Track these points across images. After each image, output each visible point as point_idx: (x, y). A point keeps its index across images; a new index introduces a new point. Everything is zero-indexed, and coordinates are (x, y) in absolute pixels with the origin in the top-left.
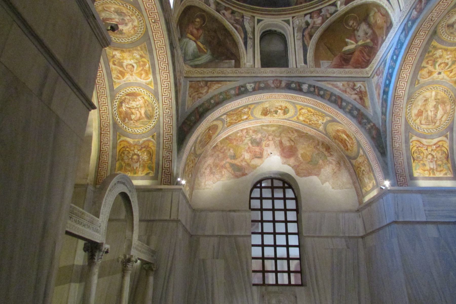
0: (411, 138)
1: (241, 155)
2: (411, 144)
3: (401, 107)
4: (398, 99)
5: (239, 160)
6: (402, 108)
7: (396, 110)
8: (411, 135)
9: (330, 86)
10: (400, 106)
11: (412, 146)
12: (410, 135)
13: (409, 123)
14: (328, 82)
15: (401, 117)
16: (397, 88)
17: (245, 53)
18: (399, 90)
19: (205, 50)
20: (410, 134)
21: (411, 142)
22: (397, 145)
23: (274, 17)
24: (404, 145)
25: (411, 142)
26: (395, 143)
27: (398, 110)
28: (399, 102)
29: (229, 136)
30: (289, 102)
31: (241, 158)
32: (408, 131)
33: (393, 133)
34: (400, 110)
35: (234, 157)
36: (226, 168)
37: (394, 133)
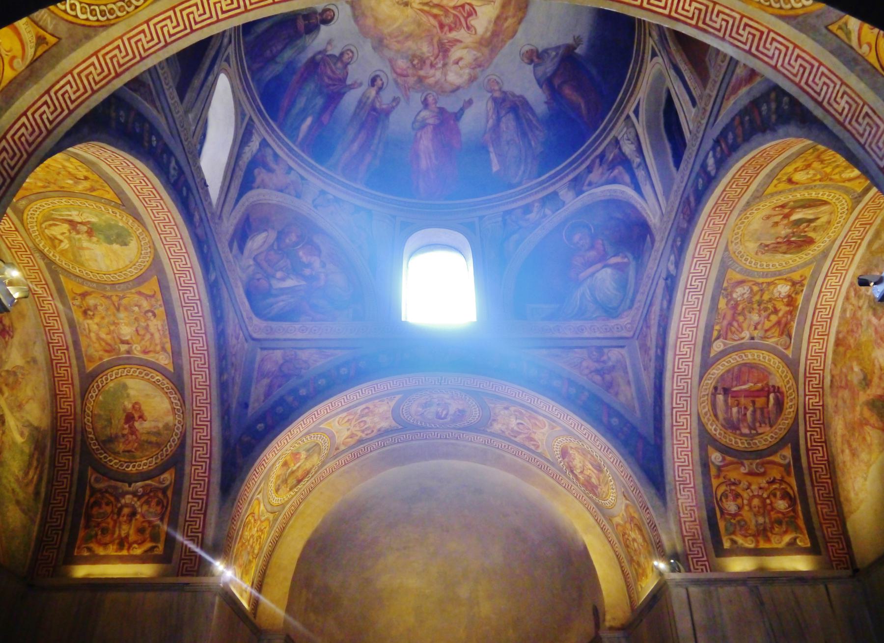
0: (848, 34)
1: (874, 365)
2: (865, 49)
3: (738, 17)
4: (711, 19)
5: (876, 380)
6: (743, 16)
7: (744, 39)
8: (840, 28)
9: (732, 101)
10: (734, 19)
11: (873, 53)
12: (839, 33)
13: (801, 12)
14: (726, 97)
15: (770, 31)
16: (673, 14)
17: (644, 205)
18: (680, 10)
19: (626, 260)
20: (834, 28)
21: (860, 45)
22: (843, 103)
23: (643, 70)
24: (853, 80)
25: (860, 45)
26: (835, 106)
27: (745, 34)
28: (719, 20)
29: (838, 332)
30: (748, 204)
31: (876, 371)
32: (824, 31)
33: (806, 87)
34: (746, 25)
35: (866, 382)
36: (867, 423)
37: (806, 83)
